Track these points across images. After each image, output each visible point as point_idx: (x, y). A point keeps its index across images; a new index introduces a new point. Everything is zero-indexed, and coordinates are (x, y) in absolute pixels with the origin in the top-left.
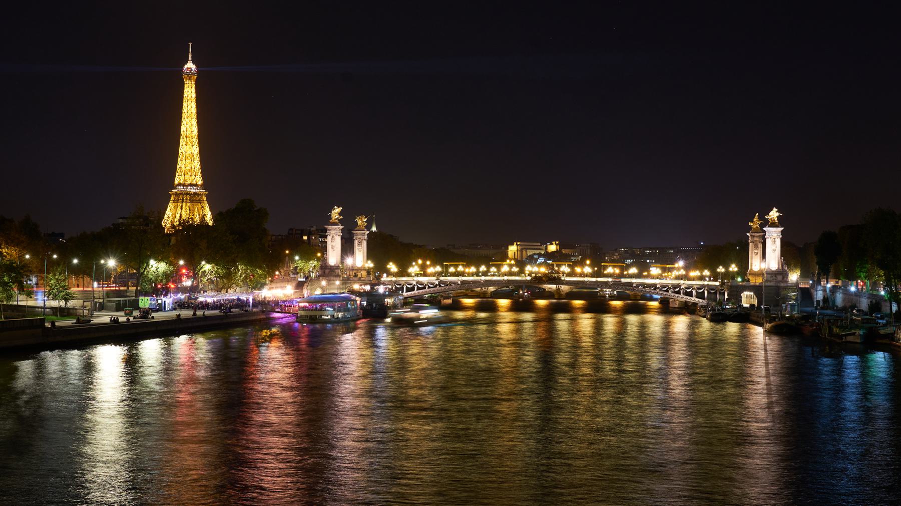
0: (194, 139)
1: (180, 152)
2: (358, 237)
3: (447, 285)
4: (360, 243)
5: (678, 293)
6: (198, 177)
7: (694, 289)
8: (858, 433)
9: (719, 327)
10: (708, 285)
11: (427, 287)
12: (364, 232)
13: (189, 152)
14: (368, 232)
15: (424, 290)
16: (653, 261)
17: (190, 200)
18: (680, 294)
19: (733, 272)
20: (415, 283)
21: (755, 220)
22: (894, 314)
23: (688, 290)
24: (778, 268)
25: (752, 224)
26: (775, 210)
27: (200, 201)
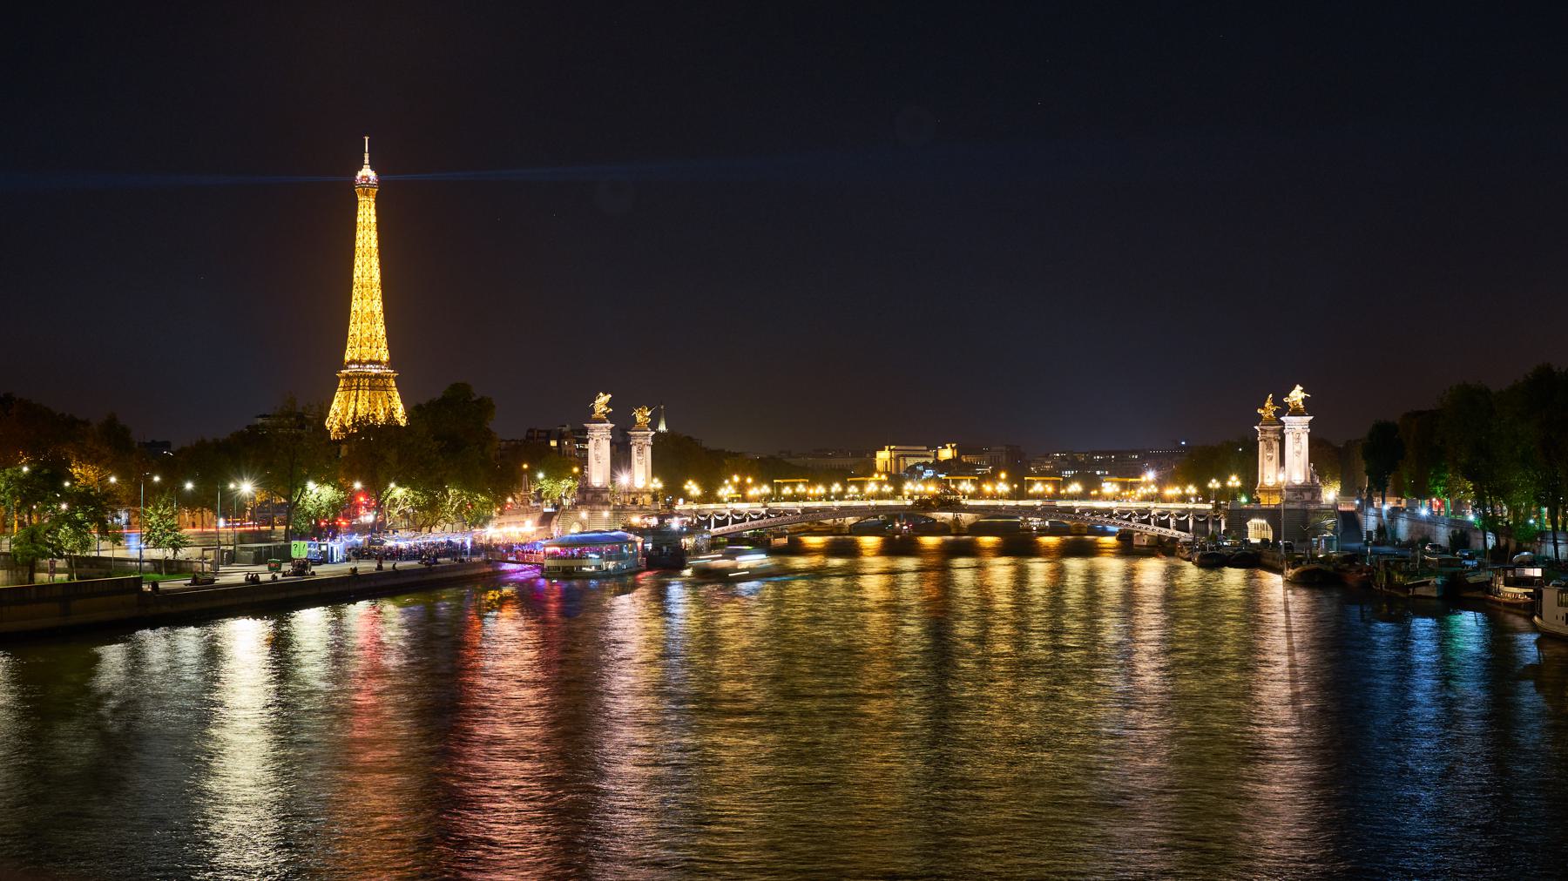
0: (375, 290)
1: (353, 310)
2: (638, 441)
3: (780, 515)
4: (640, 451)
5: (1147, 522)
6: (383, 349)
7: (1172, 516)
8: (1436, 741)
9: (1212, 575)
10: (1194, 510)
11: (748, 519)
12: (646, 433)
13: (367, 310)
14: (654, 433)
15: (742, 524)
16: (1107, 473)
17: (369, 386)
18: (1150, 524)
19: (1233, 489)
20: (729, 513)
21: (1267, 405)
22: (1490, 551)
23: (1162, 518)
24: (1305, 480)
25: (1262, 412)
26: (1299, 388)
27: (385, 388)
